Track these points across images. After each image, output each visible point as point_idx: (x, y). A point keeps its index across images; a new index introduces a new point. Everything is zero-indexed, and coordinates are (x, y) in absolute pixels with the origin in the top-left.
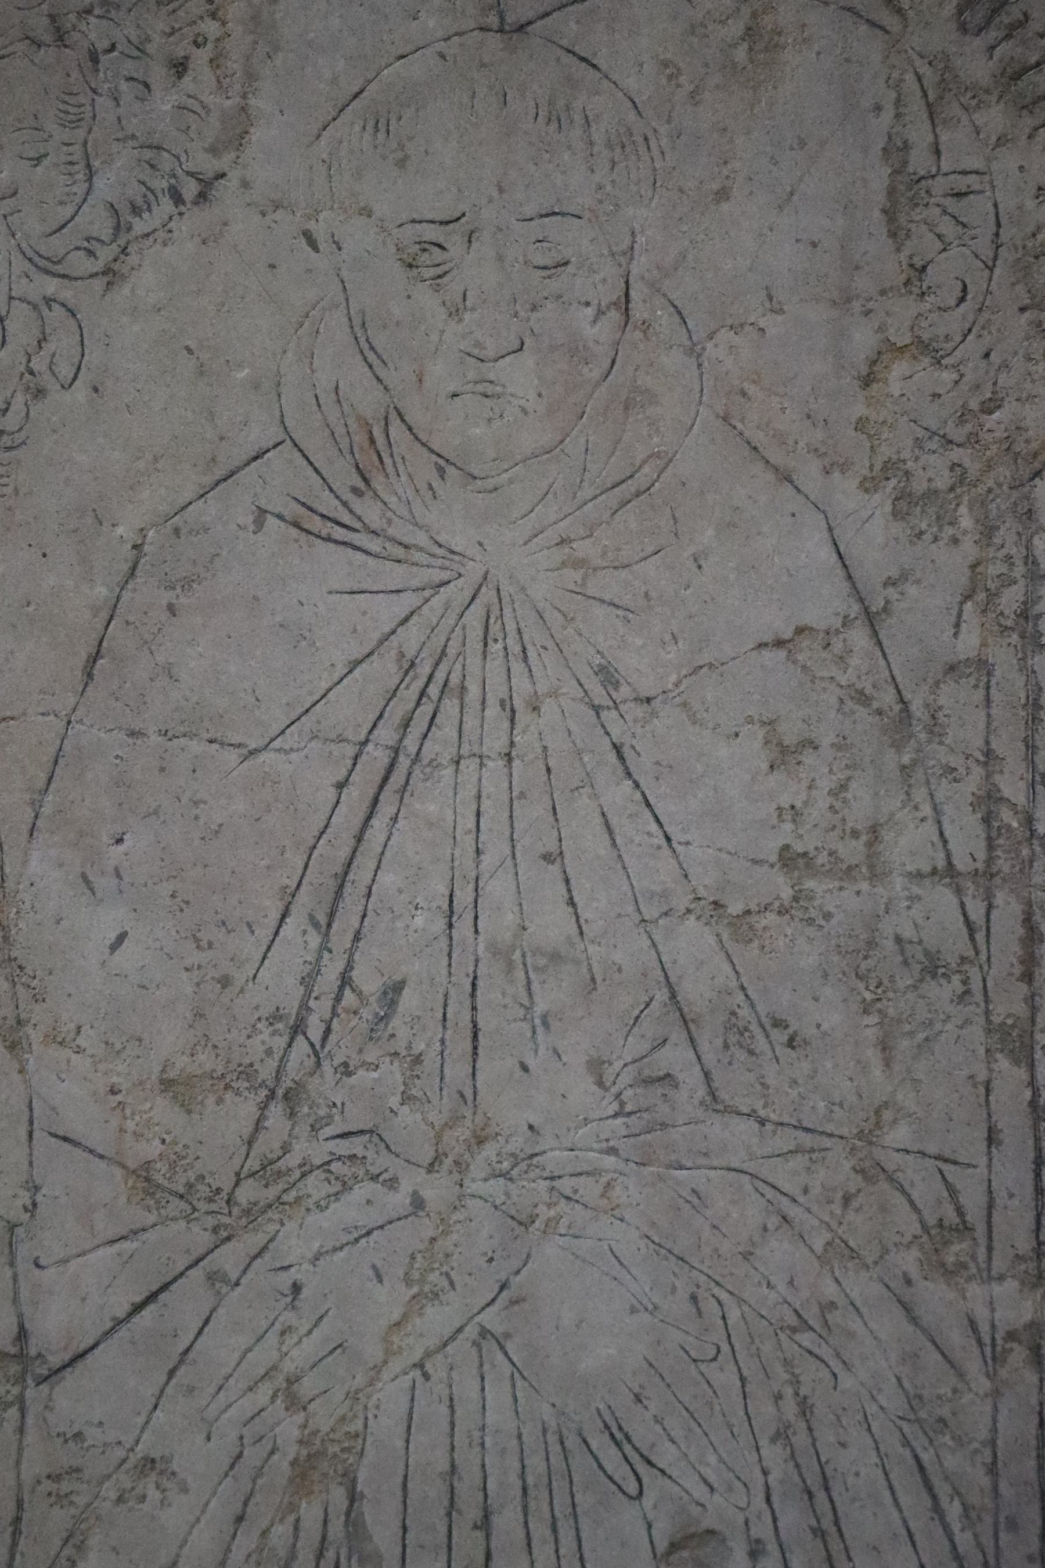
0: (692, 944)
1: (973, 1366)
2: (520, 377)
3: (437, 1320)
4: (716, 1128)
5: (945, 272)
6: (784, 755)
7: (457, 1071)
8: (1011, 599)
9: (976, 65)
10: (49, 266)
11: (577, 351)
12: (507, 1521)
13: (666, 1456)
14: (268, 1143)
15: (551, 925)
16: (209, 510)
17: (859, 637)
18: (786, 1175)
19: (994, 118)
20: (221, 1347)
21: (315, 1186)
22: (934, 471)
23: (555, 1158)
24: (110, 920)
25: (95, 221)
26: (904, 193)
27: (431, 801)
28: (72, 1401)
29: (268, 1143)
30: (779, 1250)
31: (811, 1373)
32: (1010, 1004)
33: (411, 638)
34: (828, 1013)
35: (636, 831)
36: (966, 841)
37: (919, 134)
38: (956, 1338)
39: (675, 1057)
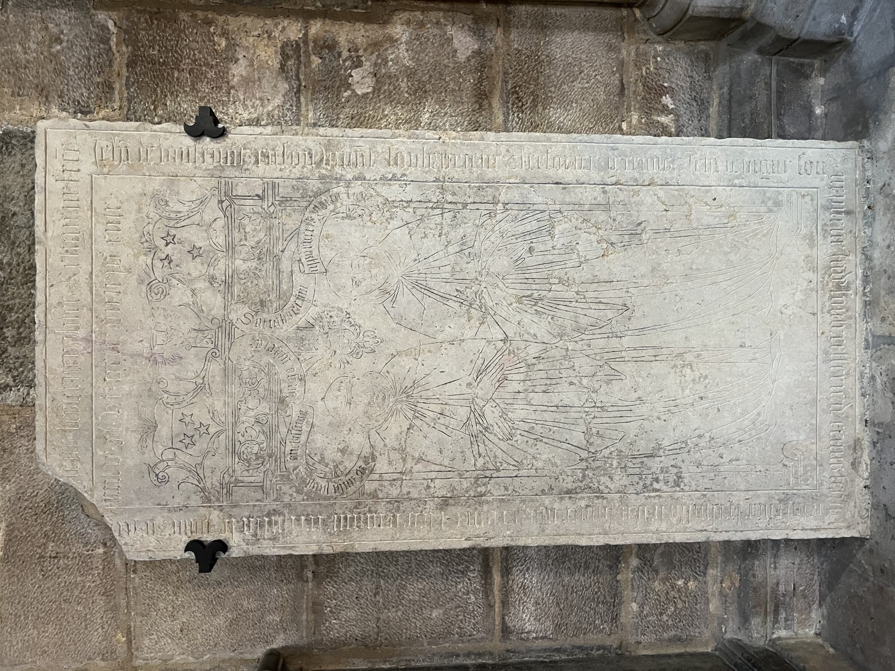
0: (451, 249)
1: (508, 212)
2: (374, 271)
3: (501, 285)
4: (476, 247)
5: (360, 212)
6: (426, 236)
7: (468, 282)
8: (405, 204)
9: (331, 207)
10: (359, 334)
11: (370, 263)
12: (527, 276)
13: (519, 254)
14: (477, 307)
15: (449, 268)
16: (392, 314)
17: (410, 225)
18: (482, 237)
19: (339, 205)
20: (504, 314)
21: (483, 301)
22: (387, 215)
23: (480, 269)
24: (447, 328)
25: (352, 329)
26: (349, 217)
27: (431, 284)
28: (511, 335)
29: (477, 307)
30: (492, 239)
31: (509, 235)
32: (460, 206)
33: (409, 287)
34: (461, 231)
35: (436, 257)
36: (438, 211)
37: (341, 215)
38: (504, 215)
39: (466, 252)
